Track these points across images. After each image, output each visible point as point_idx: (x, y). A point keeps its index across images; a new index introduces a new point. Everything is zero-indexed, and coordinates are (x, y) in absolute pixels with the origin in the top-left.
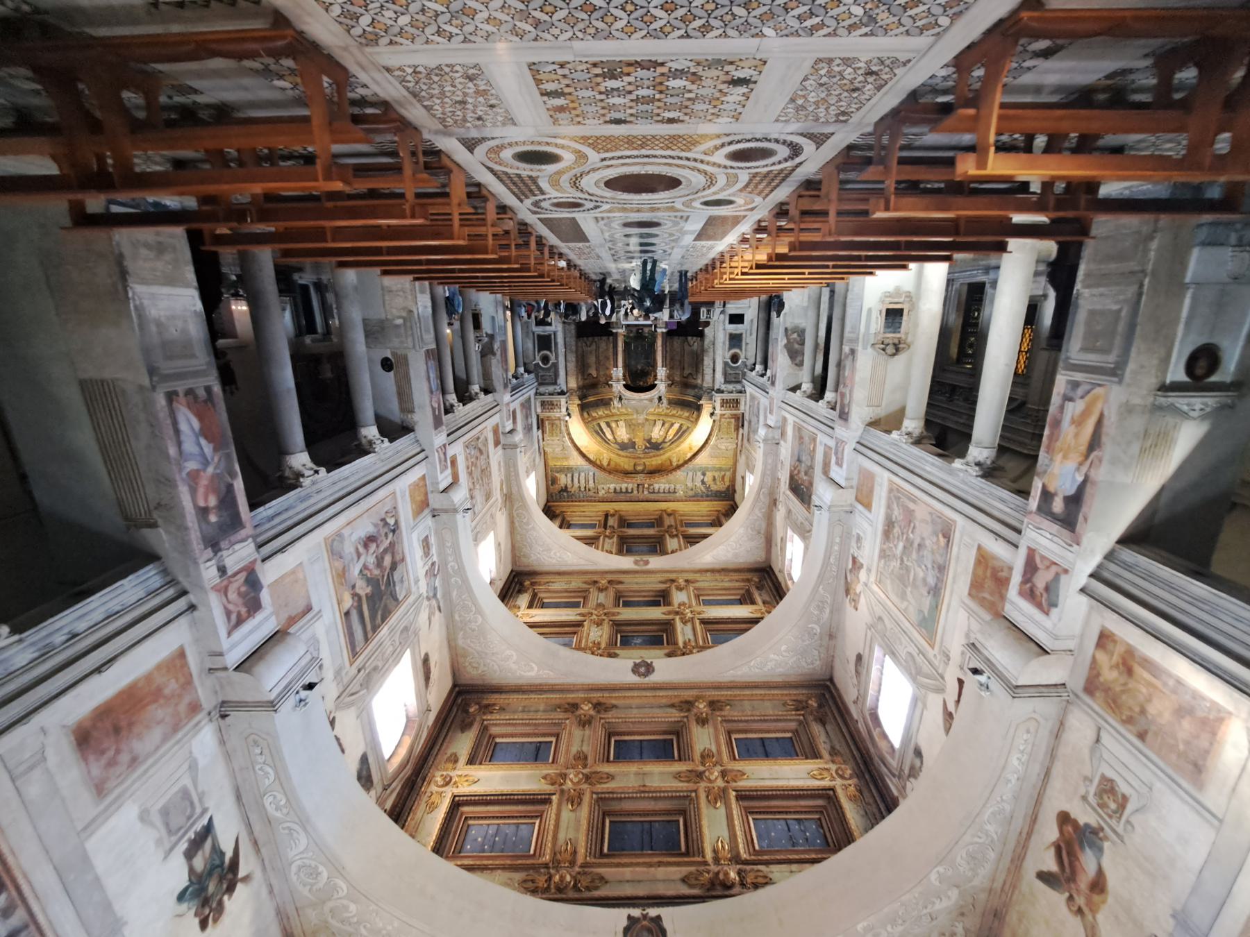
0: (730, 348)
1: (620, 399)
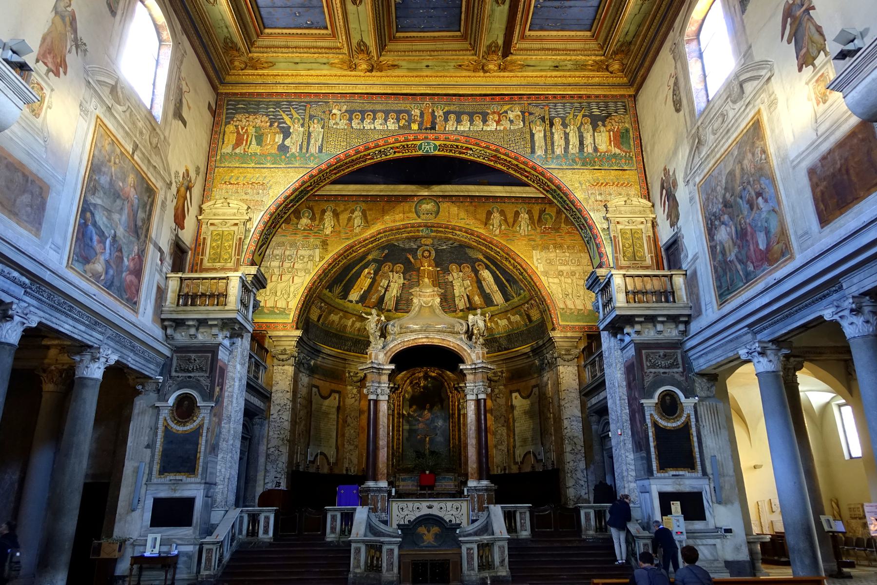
0: (197, 432)
1: (469, 334)
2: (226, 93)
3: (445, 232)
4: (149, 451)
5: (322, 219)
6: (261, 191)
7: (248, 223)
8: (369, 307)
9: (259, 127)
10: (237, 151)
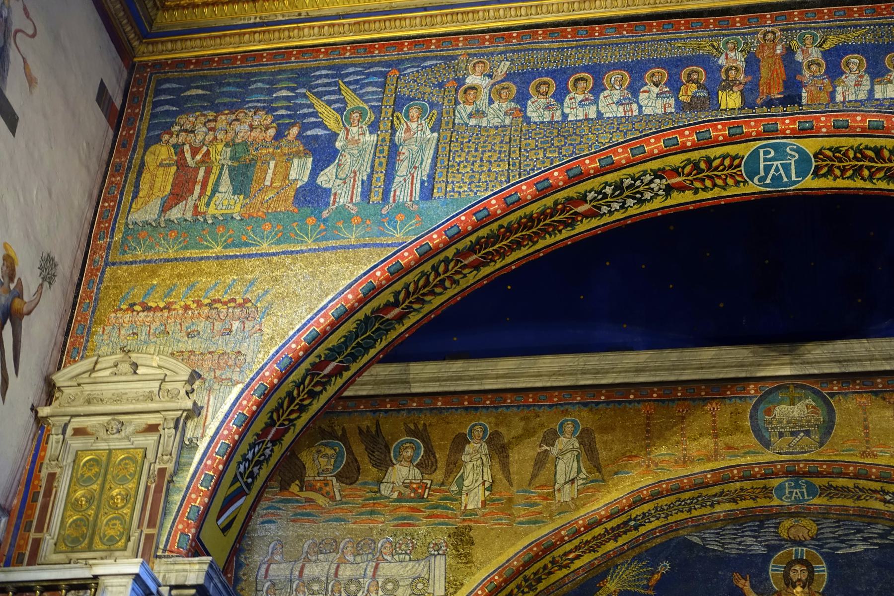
2: (158, 66)
3: (858, 493)
5: (454, 465)
6: (236, 325)
7: (190, 424)
9: (245, 143)
10: (175, 214)
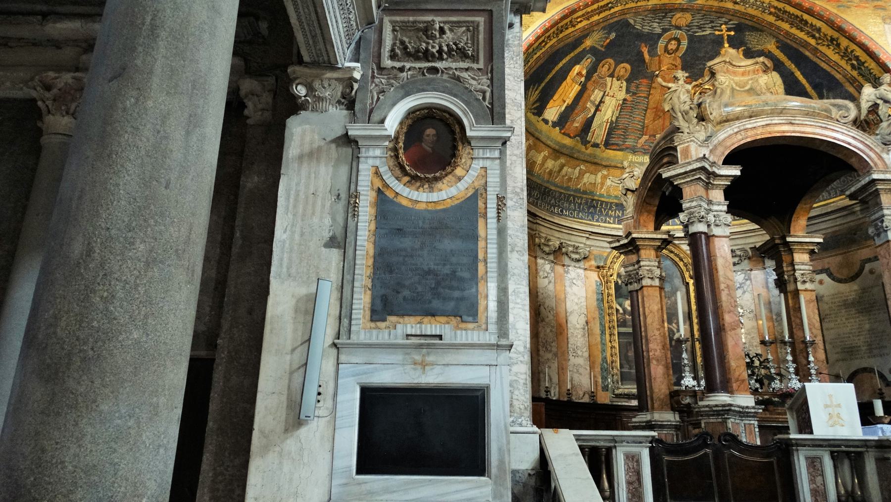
4: (335, 254)
8: (569, 136)
